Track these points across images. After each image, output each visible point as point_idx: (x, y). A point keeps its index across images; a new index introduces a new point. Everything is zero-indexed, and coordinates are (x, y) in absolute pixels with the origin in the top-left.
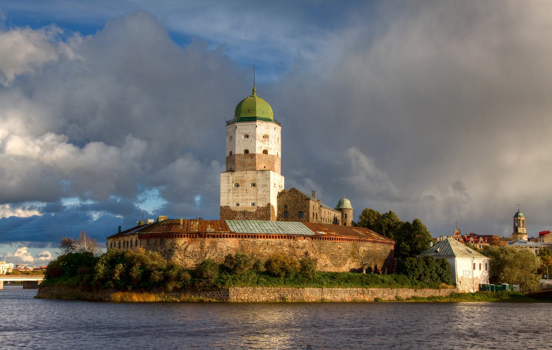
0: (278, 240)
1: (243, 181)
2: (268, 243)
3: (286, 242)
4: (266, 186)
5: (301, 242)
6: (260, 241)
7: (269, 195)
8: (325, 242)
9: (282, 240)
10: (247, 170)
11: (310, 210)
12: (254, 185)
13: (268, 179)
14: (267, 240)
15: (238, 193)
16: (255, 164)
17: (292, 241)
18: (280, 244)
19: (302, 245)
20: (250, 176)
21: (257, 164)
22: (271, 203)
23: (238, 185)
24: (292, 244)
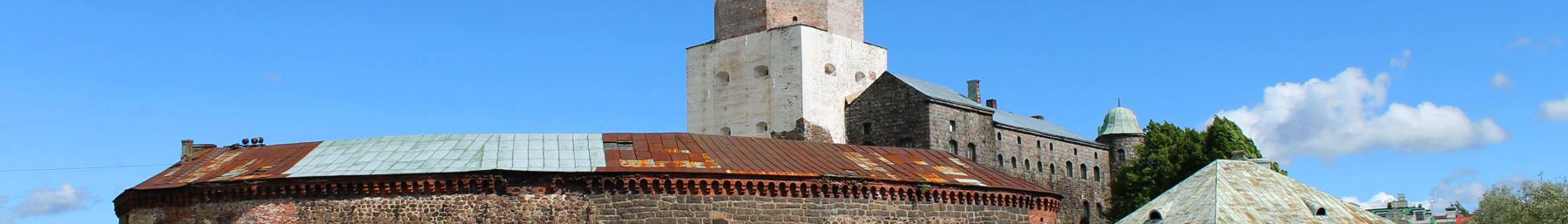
0: (437, 201)
1: (735, 65)
2: (397, 211)
3: (466, 205)
4: (791, 68)
5: (533, 201)
6: (370, 205)
7: (799, 97)
8: (645, 198)
9: (452, 198)
10: (746, 32)
11: (933, 134)
12: (764, 72)
13: (797, 48)
14: (399, 199)
15: (726, 98)
16: (765, 12)
17: (492, 199)
18: (445, 212)
19: (539, 214)
20: (750, 43)
21: (770, 12)
22: (810, 118)
23: (725, 77)
24: (493, 212)
